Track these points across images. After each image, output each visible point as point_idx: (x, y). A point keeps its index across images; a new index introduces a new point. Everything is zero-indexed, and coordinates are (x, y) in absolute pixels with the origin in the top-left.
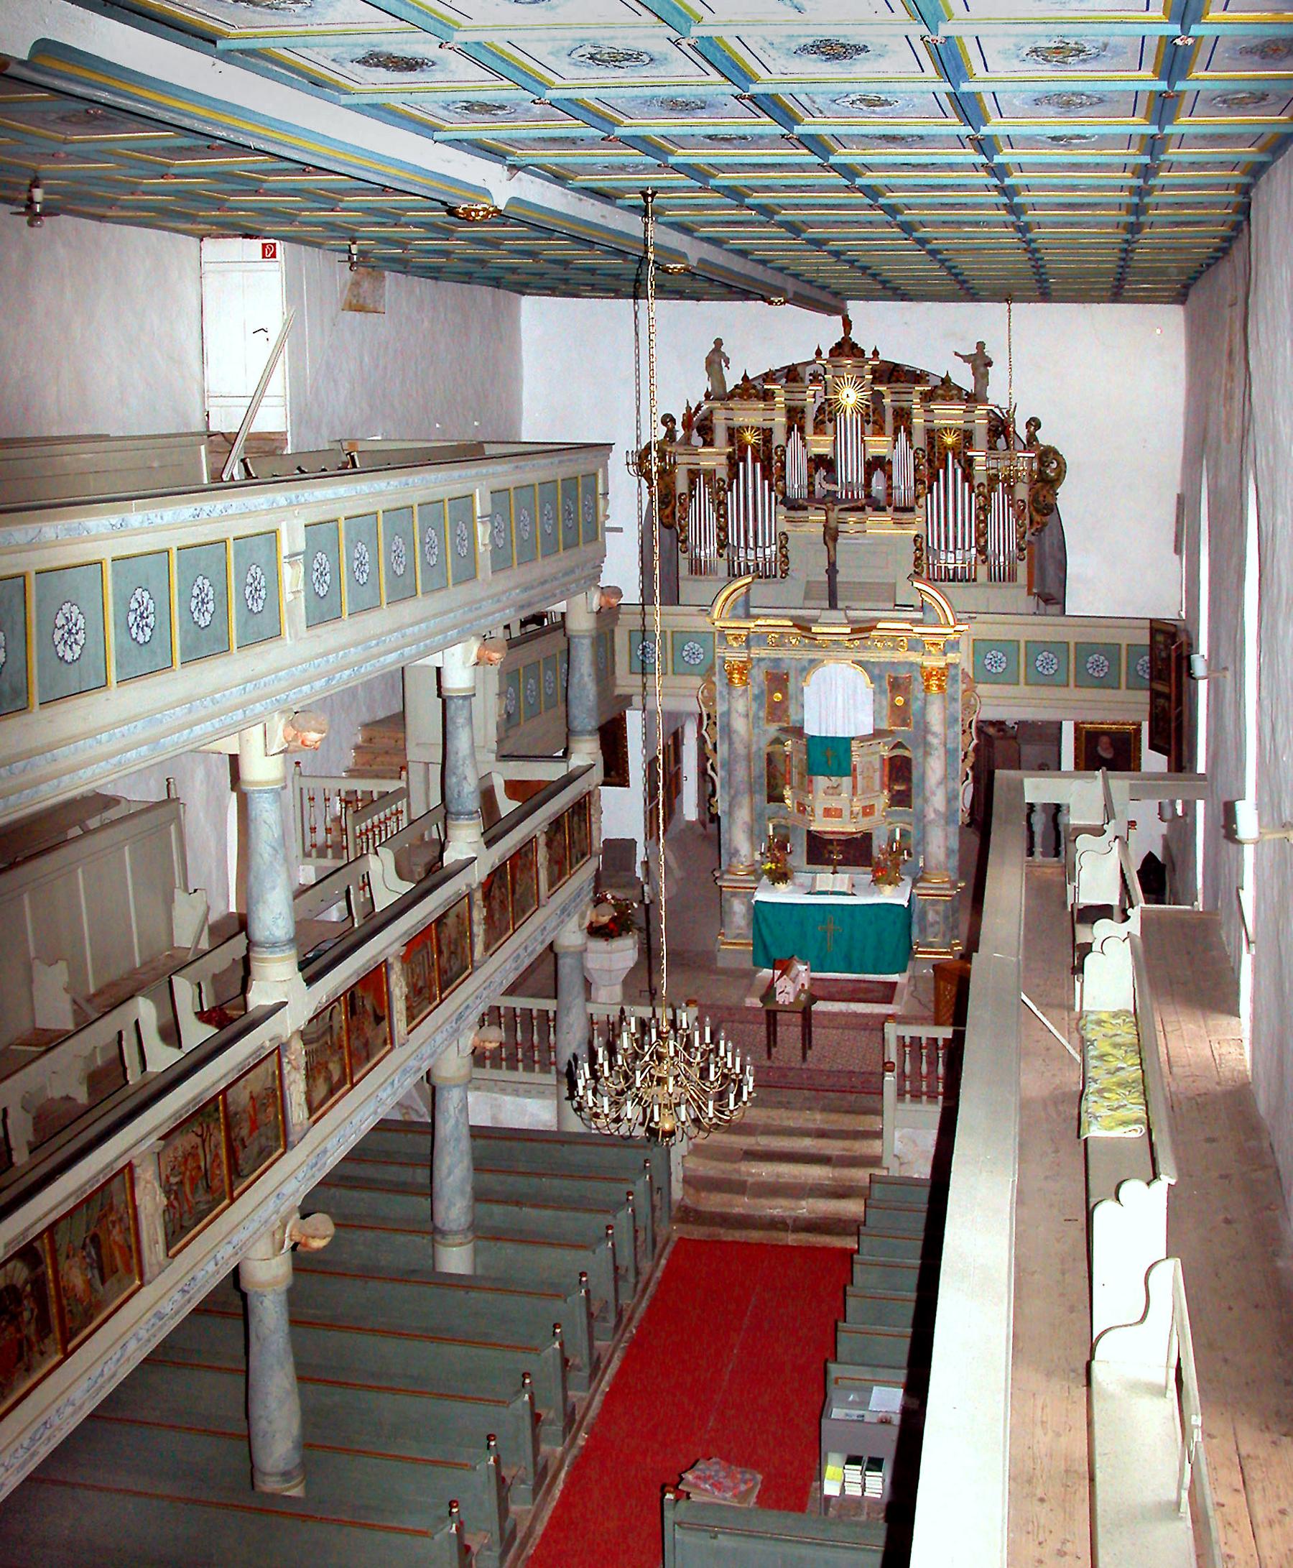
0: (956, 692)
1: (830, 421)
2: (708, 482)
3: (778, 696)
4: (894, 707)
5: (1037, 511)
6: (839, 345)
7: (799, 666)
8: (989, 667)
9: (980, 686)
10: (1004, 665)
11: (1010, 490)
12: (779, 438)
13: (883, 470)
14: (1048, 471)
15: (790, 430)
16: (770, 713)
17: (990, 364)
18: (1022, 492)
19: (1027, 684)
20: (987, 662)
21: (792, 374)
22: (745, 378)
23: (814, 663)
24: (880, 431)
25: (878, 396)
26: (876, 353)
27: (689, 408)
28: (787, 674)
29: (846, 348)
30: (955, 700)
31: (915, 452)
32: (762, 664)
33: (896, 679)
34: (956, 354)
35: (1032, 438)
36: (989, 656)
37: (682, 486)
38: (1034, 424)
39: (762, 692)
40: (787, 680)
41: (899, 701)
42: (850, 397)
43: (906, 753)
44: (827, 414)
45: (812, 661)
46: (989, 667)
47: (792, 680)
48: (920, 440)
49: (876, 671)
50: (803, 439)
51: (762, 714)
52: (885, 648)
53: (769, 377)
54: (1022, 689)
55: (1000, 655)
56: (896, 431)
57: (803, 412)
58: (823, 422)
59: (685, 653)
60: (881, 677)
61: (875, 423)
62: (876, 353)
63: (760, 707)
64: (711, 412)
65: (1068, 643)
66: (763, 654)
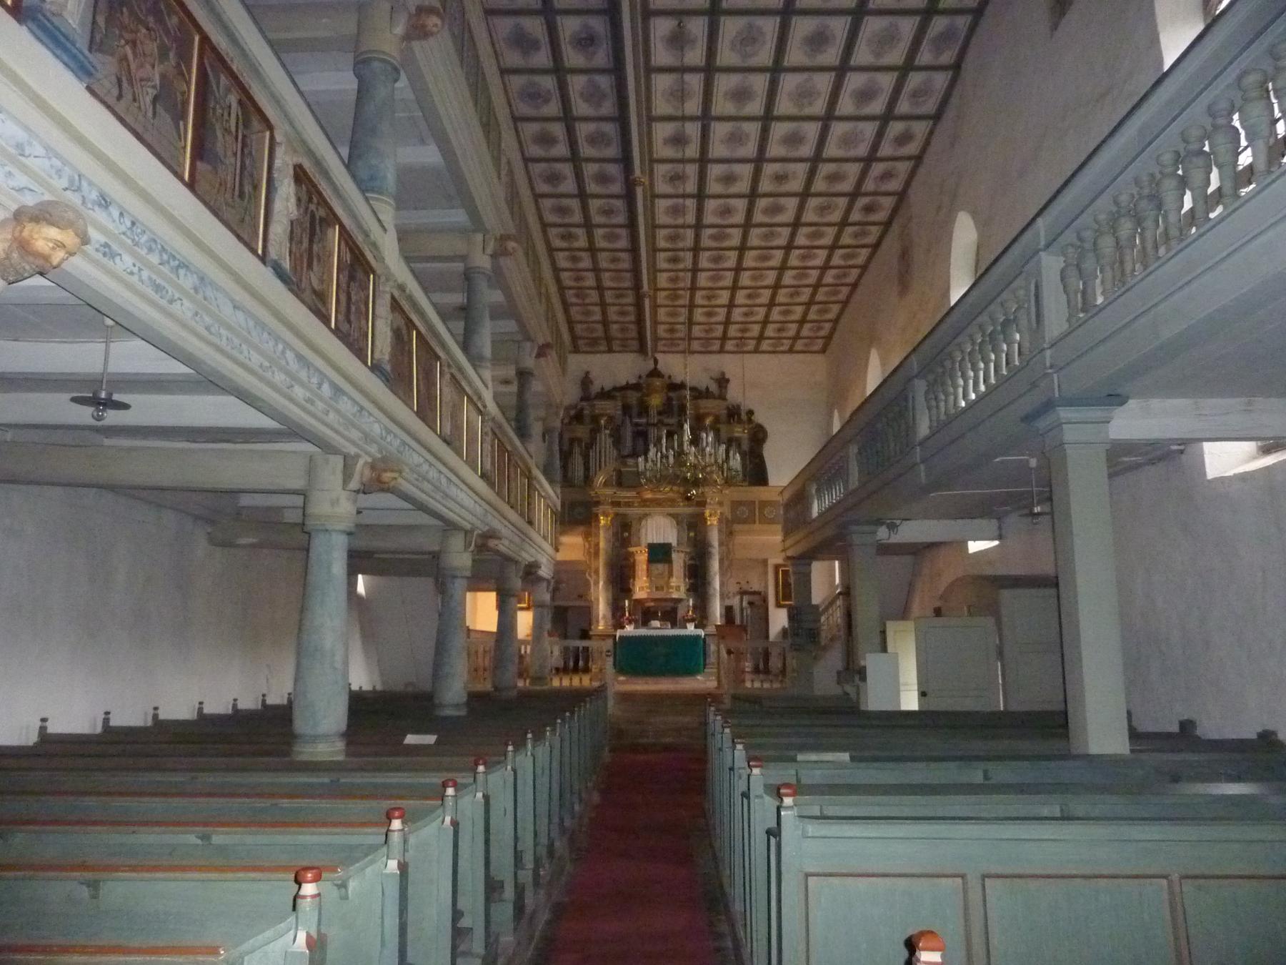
2: (580, 446)
11: (739, 446)
14: (759, 436)
17: (728, 381)
21: (628, 387)
23: (646, 516)
25: (669, 399)
29: (655, 373)
35: (750, 421)
38: (751, 413)
41: (692, 534)
42: (656, 401)
44: (644, 409)
53: (615, 389)
64: (582, 409)
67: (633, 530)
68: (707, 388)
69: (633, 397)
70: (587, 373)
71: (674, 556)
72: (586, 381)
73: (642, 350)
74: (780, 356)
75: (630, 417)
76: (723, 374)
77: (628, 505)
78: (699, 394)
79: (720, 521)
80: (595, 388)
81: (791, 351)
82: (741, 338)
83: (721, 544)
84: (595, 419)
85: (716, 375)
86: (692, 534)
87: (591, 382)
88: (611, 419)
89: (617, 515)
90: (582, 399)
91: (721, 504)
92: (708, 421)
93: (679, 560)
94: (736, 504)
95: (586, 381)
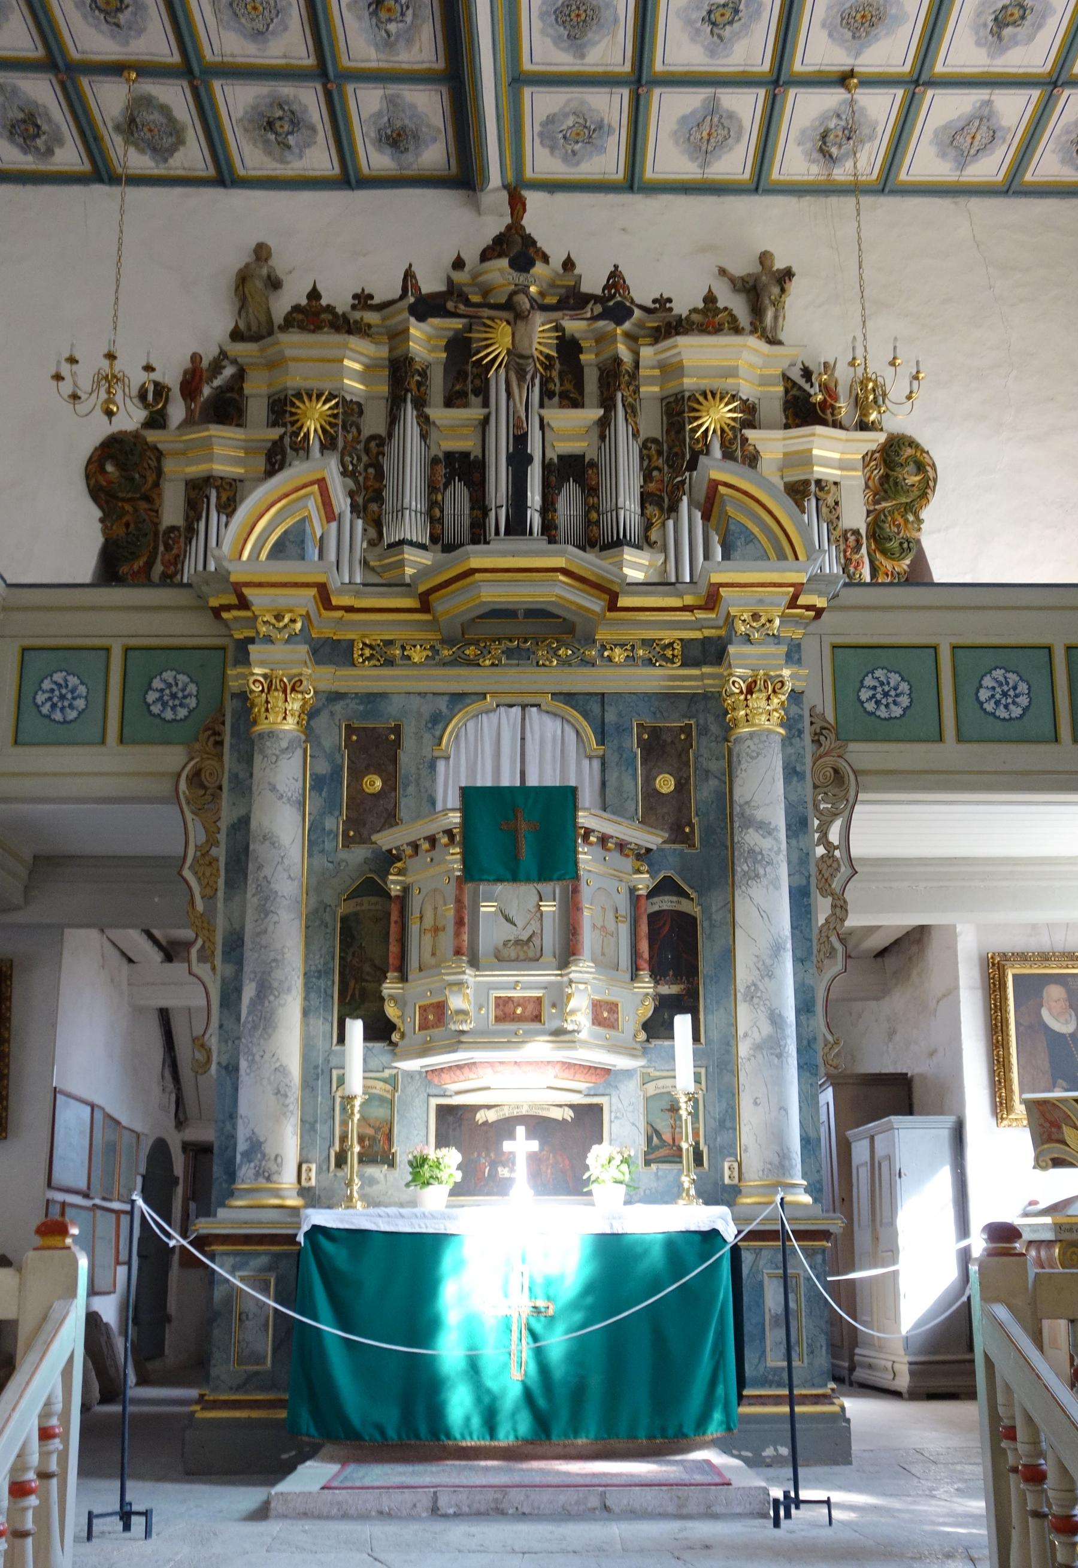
0: (800, 757)
1: (476, 392)
3: (374, 783)
4: (651, 795)
5: (884, 552)
6: (499, 240)
7: (427, 710)
8: (870, 706)
9: (853, 746)
10: (905, 701)
12: (374, 423)
13: (581, 481)
15: (395, 403)
16: (349, 823)
18: (855, 515)
19: (960, 739)
20: (865, 695)
22: (314, 295)
24: (577, 403)
25: (569, 347)
26: (568, 264)
27: (195, 358)
28: (397, 730)
30: (801, 776)
31: (644, 446)
32: (338, 707)
33: (655, 732)
34: (723, 272)
36: (869, 681)
37: (172, 513)
39: (337, 771)
40: (398, 743)
43: (685, 906)
45: (458, 699)
46: (870, 706)
47: (408, 742)
48: (651, 424)
49: (610, 717)
50: (424, 421)
51: (335, 823)
52: (631, 660)
54: (951, 752)
55: (894, 678)
56: (607, 403)
57: (423, 374)
58: (463, 394)
59: (151, 697)
60: (622, 730)
61: (564, 396)
62: (568, 264)
63: (331, 806)
64: (240, 375)
65: (1049, 649)
66: (342, 687)
67: (406, 758)
68: (710, 299)
69: (423, 340)
70: (262, 252)
71: (586, 856)
72: (255, 279)
73: (464, 176)
74: (976, 204)
75: (420, 404)
76: (765, 258)
77: (384, 655)
78: (667, 324)
79: (790, 723)
80: (293, 295)
81: (1013, 187)
82: (844, 79)
83: (797, 825)
84: (282, 408)
85: (743, 266)
86: (666, 784)
87: (274, 284)
88: (349, 412)
89: (335, 697)
90: (236, 335)
91: (794, 654)
92: (716, 417)
93: (606, 885)
94: (852, 659)
95: (255, 279)
